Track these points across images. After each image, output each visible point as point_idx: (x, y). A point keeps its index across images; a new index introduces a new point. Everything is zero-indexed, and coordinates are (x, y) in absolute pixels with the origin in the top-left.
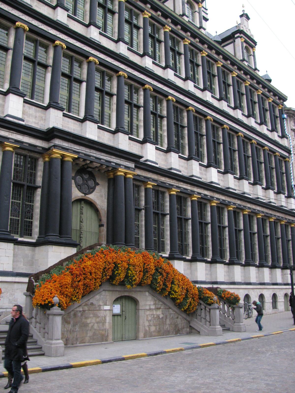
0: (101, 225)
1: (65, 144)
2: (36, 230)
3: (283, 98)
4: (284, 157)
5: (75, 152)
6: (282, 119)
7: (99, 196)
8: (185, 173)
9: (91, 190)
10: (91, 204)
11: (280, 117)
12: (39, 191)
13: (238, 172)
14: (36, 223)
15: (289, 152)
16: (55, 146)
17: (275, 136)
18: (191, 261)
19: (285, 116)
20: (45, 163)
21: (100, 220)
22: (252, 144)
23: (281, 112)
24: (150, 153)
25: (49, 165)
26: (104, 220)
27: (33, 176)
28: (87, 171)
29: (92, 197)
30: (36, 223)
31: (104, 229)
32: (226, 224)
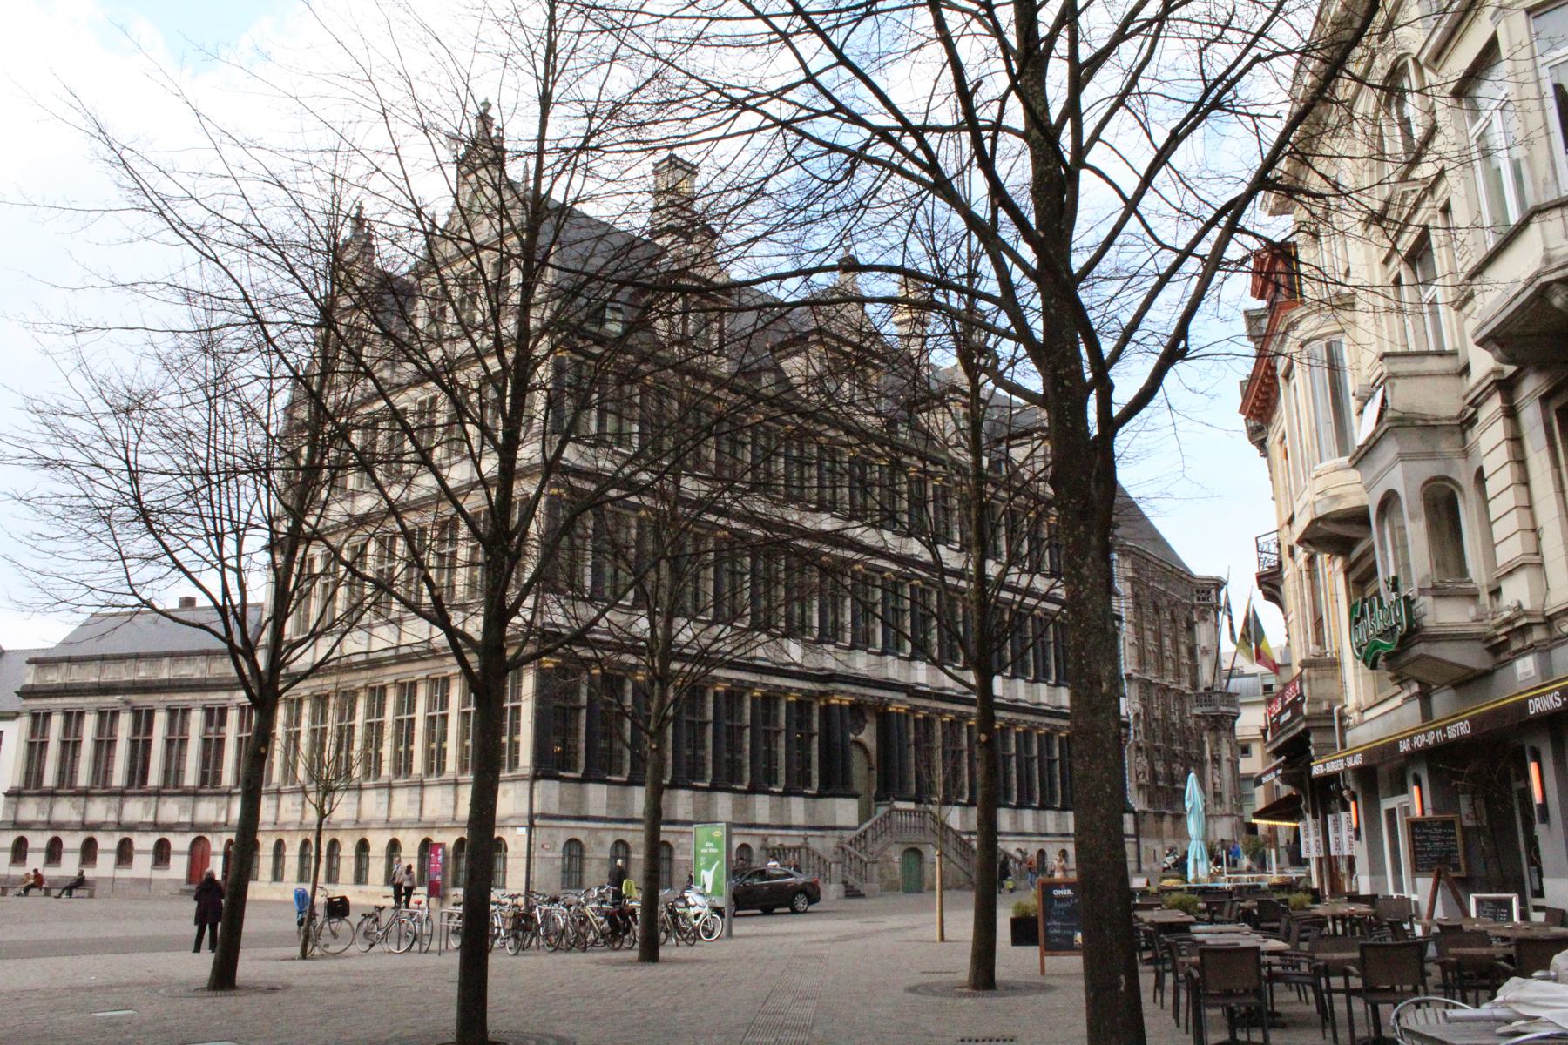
0: (870, 769)
1: (843, 687)
2: (816, 781)
5: (853, 694)
7: (868, 736)
9: (861, 729)
10: (860, 744)
12: (816, 739)
13: (1032, 671)
14: (815, 773)
16: (834, 691)
18: (966, 805)
19: (1115, 556)
25: (826, 711)
27: (809, 722)
28: (858, 710)
29: (863, 737)
30: (815, 773)
31: (875, 772)
32: (1013, 750)
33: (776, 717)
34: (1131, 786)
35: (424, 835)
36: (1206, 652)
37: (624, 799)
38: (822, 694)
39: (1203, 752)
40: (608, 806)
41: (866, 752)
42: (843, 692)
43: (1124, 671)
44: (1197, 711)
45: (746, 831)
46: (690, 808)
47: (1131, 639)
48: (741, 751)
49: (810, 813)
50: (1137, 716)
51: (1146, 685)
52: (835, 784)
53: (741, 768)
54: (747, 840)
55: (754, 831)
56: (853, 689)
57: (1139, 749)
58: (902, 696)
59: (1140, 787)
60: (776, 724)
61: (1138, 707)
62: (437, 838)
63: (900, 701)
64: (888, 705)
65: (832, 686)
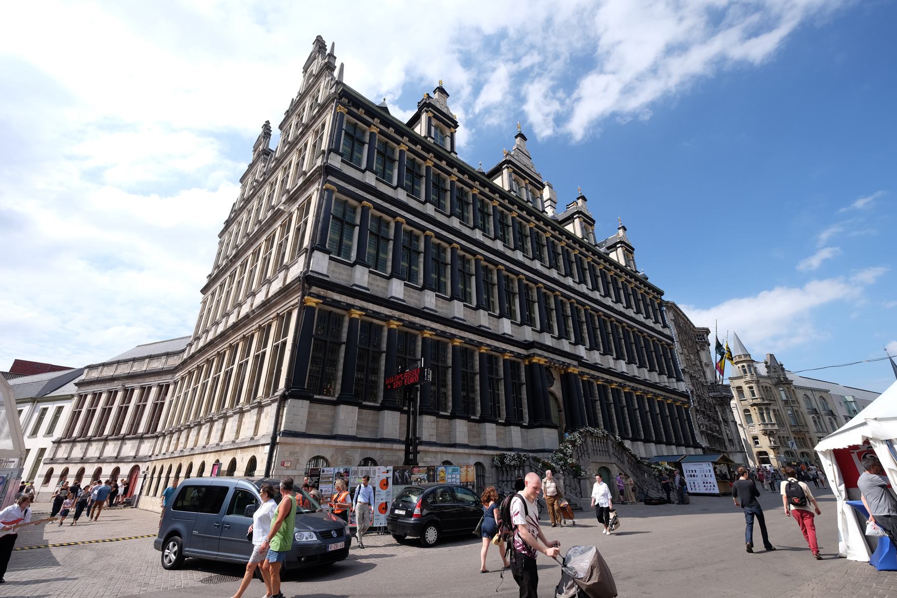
0: (560, 411)
1: (540, 352)
3: (661, 293)
4: (668, 345)
8: (605, 366)
10: (552, 394)
11: (660, 309)
12: (524, 387)
14: (526, 411)
15: (672, 340)
16: (534, 354)
17: (659, 327)
20: (525, 366)
21: (559, 407)
22: (644, 337)
23: (660, 305)
24: (581, 351)
26: (562, 406)
29: (552, 389)
30: (526, 411)
32: (637, 406)
33: (497, 370)
34: (696, 432)
36: (707, 365)
37: (377, 421)
39: (718, 417)
40: (358, 427)
41: (556, 399)
42: (540, 356)
43: (681, 367)
44: (711, 395)
45: (480, 451)
46: (434, 432)
47: (680, 351)
48: (474, 391)
49: (524, 440)
50: (692, 392)
51: (691, 377)
52: (539, 420)
53: (474, 403)
54: (481, 460)
55: (486, 452)
56: (546, 354)
57: (697, 411)
58: (575, 363)
59: (702, 433)
60: (497, 374)
61: (691, 386)
63: (575, 366)
65: (532, 351)
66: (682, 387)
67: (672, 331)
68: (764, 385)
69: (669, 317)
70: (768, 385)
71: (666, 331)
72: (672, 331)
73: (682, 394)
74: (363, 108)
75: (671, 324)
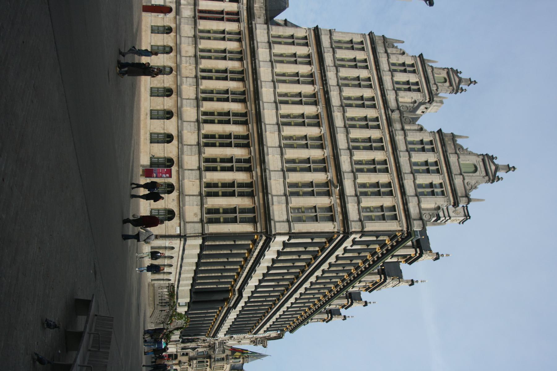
1: (237, 296)
6: (277, 330)
15: (255, 333)
17: (265, 328)
19: (279, 333)
20: (229, 287)
35: (175, 160)
38: (234, 290)
43: (235, 336)
58: (231, 306)
62: (174, 169)
64: (228, 303)
66: (221, 335)
67: (261, 334)
68: (225, 367)
69: (273, 334)
70: (224, 369)
71: (262, 331)
72: (261, 334)
73: (214, 336)
74: (396, 245)
75: (267, 334)
